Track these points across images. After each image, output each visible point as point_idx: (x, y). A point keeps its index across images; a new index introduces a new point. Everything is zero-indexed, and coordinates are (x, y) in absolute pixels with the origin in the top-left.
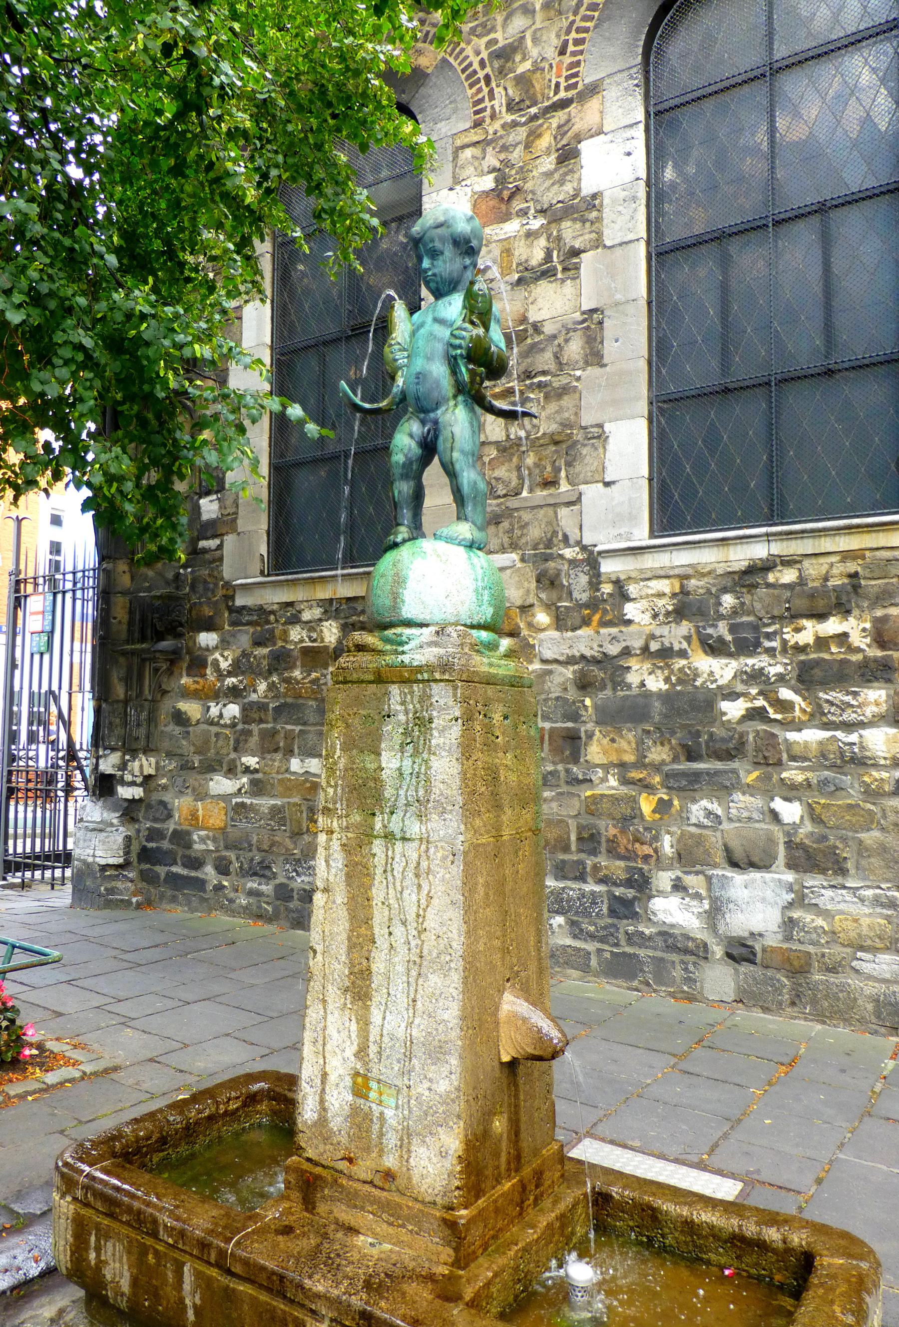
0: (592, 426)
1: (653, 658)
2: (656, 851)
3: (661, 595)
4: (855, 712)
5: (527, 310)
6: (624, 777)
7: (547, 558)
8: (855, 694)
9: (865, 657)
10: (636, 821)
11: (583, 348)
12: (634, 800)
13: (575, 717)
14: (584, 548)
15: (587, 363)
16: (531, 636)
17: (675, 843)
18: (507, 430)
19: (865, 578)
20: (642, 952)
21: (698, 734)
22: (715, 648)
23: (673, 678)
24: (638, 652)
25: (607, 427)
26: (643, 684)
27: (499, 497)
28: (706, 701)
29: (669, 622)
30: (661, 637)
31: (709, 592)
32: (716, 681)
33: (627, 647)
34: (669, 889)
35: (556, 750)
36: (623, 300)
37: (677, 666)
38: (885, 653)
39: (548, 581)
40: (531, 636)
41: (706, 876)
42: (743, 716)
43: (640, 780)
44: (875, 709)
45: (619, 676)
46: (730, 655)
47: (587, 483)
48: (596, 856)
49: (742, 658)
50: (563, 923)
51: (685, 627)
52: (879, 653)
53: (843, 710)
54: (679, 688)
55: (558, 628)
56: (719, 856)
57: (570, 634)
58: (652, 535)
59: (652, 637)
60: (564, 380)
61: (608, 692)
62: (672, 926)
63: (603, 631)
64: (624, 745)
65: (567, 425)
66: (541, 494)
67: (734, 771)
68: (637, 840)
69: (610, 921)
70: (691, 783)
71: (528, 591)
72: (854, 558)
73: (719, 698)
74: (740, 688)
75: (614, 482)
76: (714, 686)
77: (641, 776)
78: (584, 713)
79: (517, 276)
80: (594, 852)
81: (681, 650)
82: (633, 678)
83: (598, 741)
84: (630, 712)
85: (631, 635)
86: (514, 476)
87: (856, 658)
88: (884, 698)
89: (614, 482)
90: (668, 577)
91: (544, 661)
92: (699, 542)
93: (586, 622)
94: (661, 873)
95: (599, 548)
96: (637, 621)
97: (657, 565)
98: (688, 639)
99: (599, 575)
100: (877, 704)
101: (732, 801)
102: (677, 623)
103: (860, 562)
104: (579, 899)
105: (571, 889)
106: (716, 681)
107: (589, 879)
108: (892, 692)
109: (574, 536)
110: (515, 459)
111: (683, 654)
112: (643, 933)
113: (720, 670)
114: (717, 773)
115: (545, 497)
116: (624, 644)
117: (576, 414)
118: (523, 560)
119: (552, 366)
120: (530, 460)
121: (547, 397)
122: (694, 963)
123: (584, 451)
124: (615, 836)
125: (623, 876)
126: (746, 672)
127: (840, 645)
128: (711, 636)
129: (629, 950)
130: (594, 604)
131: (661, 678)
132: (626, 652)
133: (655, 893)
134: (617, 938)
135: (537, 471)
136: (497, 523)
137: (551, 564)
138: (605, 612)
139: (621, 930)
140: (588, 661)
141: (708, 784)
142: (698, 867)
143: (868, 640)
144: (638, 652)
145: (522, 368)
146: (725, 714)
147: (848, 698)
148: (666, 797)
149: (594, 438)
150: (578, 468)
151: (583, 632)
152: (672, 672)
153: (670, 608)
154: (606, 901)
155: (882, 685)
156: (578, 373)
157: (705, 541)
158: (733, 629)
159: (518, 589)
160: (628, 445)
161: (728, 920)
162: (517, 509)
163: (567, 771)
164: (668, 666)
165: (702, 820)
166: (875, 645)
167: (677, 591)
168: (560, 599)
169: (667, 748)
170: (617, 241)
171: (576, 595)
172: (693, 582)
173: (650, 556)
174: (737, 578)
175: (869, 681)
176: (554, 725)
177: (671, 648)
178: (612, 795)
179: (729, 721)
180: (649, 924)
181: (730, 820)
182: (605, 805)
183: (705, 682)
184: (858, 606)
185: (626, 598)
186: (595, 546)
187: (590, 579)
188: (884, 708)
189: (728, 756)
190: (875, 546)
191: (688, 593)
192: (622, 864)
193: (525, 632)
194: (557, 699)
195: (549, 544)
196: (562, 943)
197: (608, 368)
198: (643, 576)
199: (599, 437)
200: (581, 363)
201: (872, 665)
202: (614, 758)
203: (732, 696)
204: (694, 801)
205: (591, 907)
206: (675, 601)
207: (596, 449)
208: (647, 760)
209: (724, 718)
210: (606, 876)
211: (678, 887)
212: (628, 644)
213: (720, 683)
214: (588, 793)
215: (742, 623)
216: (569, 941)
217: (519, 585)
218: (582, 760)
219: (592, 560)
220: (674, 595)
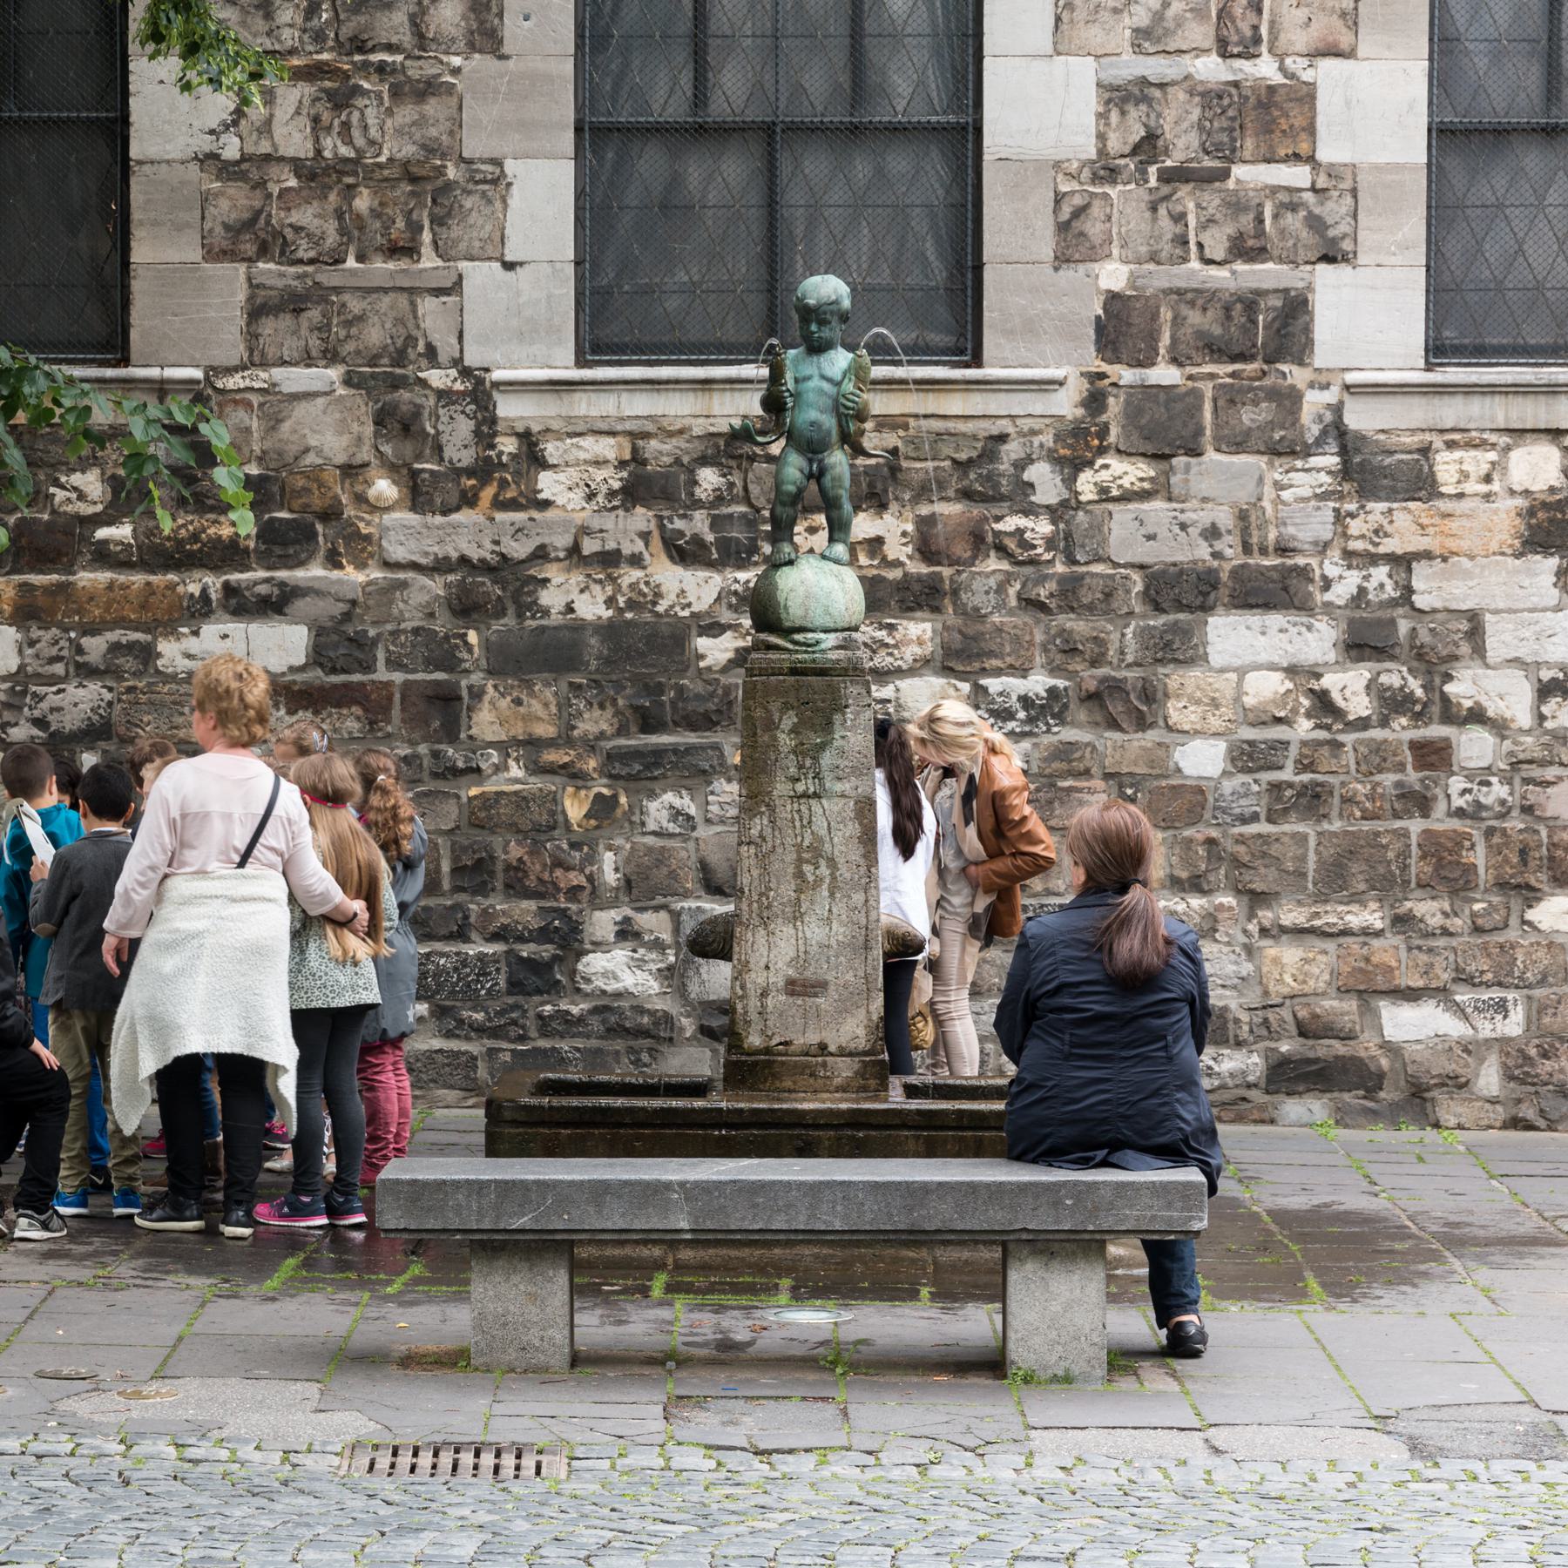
0: (483, 161)
1: (586, 564)
2: (590, 879)
3: (599, 463)
4: (891, 654)
6: (535, 762)
7: (396, 383)
8: (891, 628)
9: (906, 574)
10: (556, 833)
11: (464, 17)
12: (555, 799)
13: (449, 662)
14: (466, 372)
15: (472, 47)
16: (362, 519)
17: (620, 864)
18: (317, 140)
19: (907, 458)
20: (564, 1045)
21: (660, 689)
22: (686, 553)
23: (621, 601)
24: (562, 555)
25: (510, 166)
26: (570, 609)
27: (300, 262)
28: (672, 636)
29: (614, 508)
30: (601, 531)
31: (678, 461)
32: (689, 605)
33: (542, 547)
34: (612, 938)
35: (416, 721)
37: (625, 582)
38: (932, 569)
39: (398, 424)
40: (362, 519)
41: (670, 912)
42: (730, 661)
43: (564, 766)
44: (918, 651)
45: (529, 593)
46: (711, 565)
47: (472, 259)
48: (486, 896)
49: (729, 570)
50: (426, 1013)
51: (642, 518)
52: (925, 569)
53: (874, 652)
54: (629, 615)
55: (414, 508)
56: (690, 882)
57: (439, 519)
58: (581, 362)
59: (584, 530)
60: (431, 70)
61: (510, 621)
62: (618, 995)
63: (500, 516)
64: (537, 707)
65: (430, 149)
66: (382, 267)
67: (716, 747)
68: (558, 863)
69: (510, 1000)
70: (647, 767)
71: (359, 439)
72: (894, 427)
73: (694, 632)
74: (726, 617)
75: (521, 264)
76: (686, 613)
77: (566, 759)
78: (466, 656)
80: (482, 889)
81: (633, 555)
82: (551, 598)
83: (492, 703)
84: (549, 654)
85: (550, 525)
86: (331, 227)
87: (894, 574)
88: (929, 633)
89: (521, 264)
90: (612, 434)
91: (388, 565)
92: (668, 382)
93: (469, 500)
94: (597, 914)
95: (497, 375)
96: (560, 502)
97: (594, 413)
98: (645, 536)
99: (493, 421)
100: (920, 642)
101: (712, 793)
102: (627, 510)
103: (901, 433)
104: (456, 969)
105: (442, 955)
106: (689, 605)
107: (474, 935)
108: (939, 626)
109: (446, 346)
110: (333, 197)
111: (636, 561)
112: (568, 1012)
113: (695, 589)
114: (690, 750)
115: (392, 274)
116: (538, 541)
117: (451, 133)
118: (348, 382)
119: (406, 38)
120: (363, 202)
121: (396, 93)
122: (651, 1050)
123: (468, 203)
124: (520, 860)
125: (536, 924)
126: (736, 593)
127: (872, 554)
128: (681, 534)
129: (543, 1043)
130: (484, 470)
131: (601, 598)
132: (541, 554)
133: (588, 947)
134: (523, 1027)
135: (378, 225)
136: (297, 311)
137: (404, 395)
138: (504, 484)
139: (531, 1014)
140: (474, 567)
141: (675, 766)
142: (660, 900)
143: (909, 549)
144: (562, 555)
145: (346, 31)
146: (702, 657)
147: (881, 634)
148: (605, 791)
149: (485, 182)
150: (456, 231)
151: (463, 516)
152: (618, 589)
153: (616, 485)
154: (504, 969)
155: (927, 615)
156: (456, 61)
157: (677, 382)
158: (716, 523)
159: (341, 434)
160: (541, 200)
161: (705, 976)
162: (337, 290)
163: (436, 755)
164: (612, 579)
165: (665, 824)
166: (917, 555)
167: (628, 457)
168: (419, 457)
169: (609, 712)
171: (449, 452)
172: (654, 443)
173: (583, 395)
174: (722, 443)
175: (911, 609)
176: (411, 677)
177: (618, 551)
178: (516, 793)
179: (709, 669)
180: (577, 998)
181: (708, 821)
182: (504, 810)
183: (672, 607)
184: (897, 499)
185: (542, 463)
186: (487, 370)
187: (478, 425)
188: (929, 648)
189: (706, 722)
190: (922, 411)
191: (644, 462)
192: (531, 905)
193: (350, 512)
194: (416, 631)
195: (400, 358)
196: (425, 1047)
197: (511, 63)
198: (570, 429)
199: (495, 182)
201: (916, 587)
202: (519, 731)
203: (715, 629)
204: (652, 795)
205: (478, 981)
206: (625, 474)
207: (490, 202)
208: (576, 733)
209: (702, 664)
210: (504, 927)
211: (626, 933)
212: (547, 540)
213: (695, 608)
214: (474, 792)
215: (731, 516)
216: (437, 1043)
217: (342, 427)
218: (463, 736)
219: (479, 393)
220: (622, 464)
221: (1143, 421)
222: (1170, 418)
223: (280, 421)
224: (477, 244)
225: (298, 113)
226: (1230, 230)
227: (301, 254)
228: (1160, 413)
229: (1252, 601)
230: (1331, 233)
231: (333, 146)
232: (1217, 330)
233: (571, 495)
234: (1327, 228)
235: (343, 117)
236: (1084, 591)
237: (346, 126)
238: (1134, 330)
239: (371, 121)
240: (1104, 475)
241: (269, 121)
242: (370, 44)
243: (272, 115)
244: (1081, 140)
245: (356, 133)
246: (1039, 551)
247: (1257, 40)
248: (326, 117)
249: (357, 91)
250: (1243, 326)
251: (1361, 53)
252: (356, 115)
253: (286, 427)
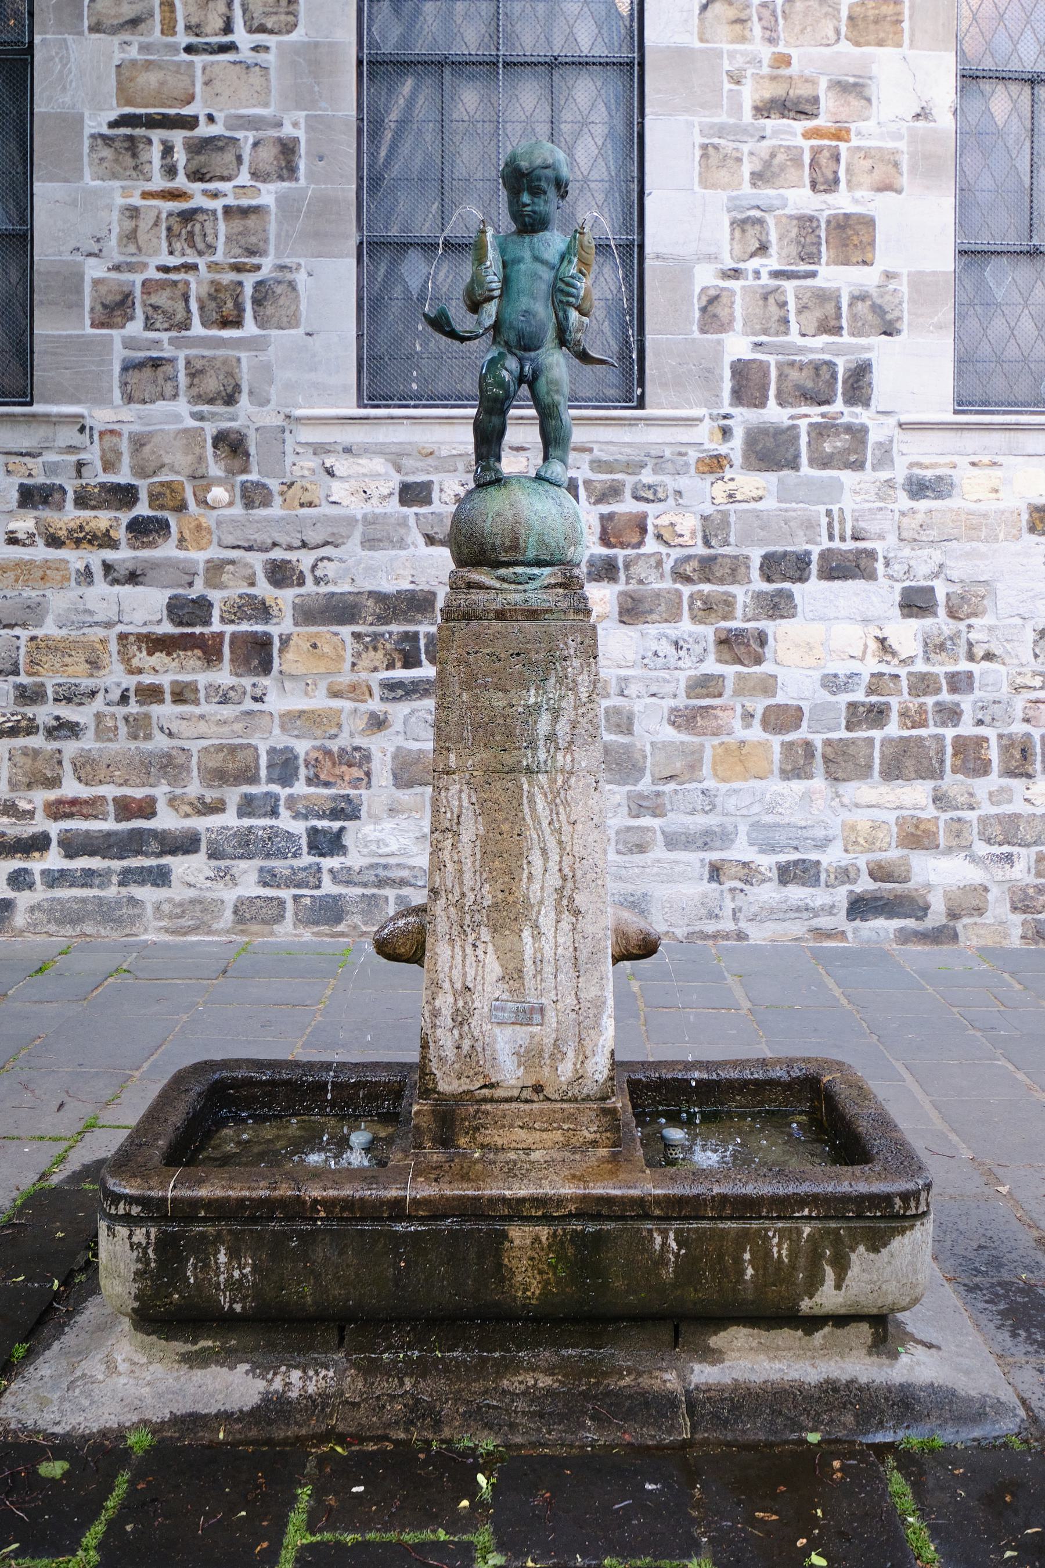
11: (276, 158)
52: (605, 551)
96: (344, 503)
104: (270, 838)
135: (213, 305)
159: (187, 454)
160: (329, 287)
221: (758, 448)
222: (777, 446)
223: (142, 445)
224: (285, 319)
225: (156, 224)
226: (818, 313)
227: (158, 325)
228: (770, 443)
229: (835, 574)
230: (889, 317)
232: (809, 384)
233: (353, 499)
234: (886, 313)
235: (189, 228)
236: (716, 568)
238: (751, 384)
240: (732, 485)
241: (135, 231)
242: (208, 176)
245: (198, 239)
246: (686, 538)
247: (836, 181)
248: (176, 228)
250: (827, 381)
252: (198, 226)
253: (147, 449)
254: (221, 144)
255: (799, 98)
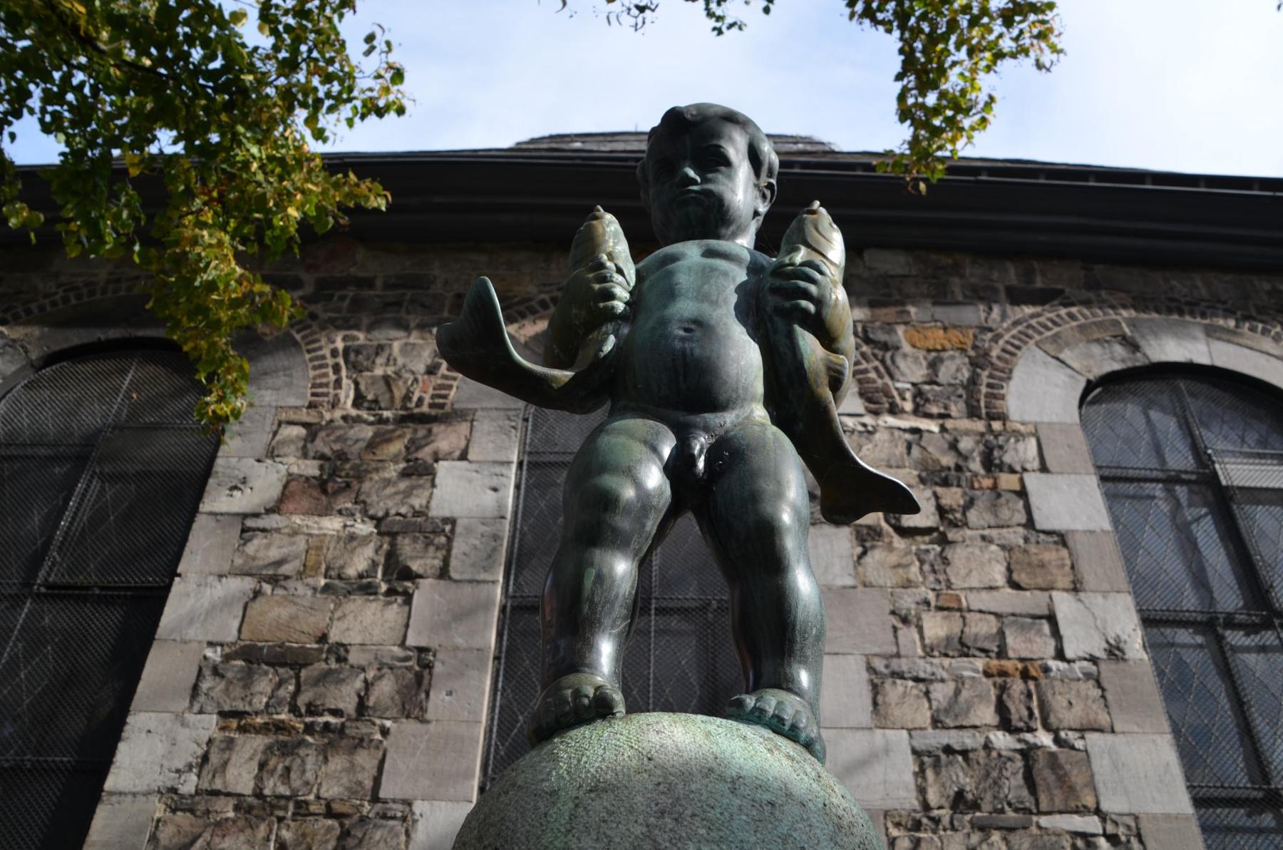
0: (394, 801)
5: (329, 626)
25: (418, 807)
36: (465, 645)
79: (323, 582)
119: (349, 705)
170: (467, 576)
197: (432, 727)
200: (394, 712)
231: (272, 786)
237: (288, 770)
239: (308, 767)
243: (229, 759)
244: (902, 794)
245: (293, 775)
249: (302, 743)
251: (1117, 728)
254: (342, 676)
255: (976, 635)
